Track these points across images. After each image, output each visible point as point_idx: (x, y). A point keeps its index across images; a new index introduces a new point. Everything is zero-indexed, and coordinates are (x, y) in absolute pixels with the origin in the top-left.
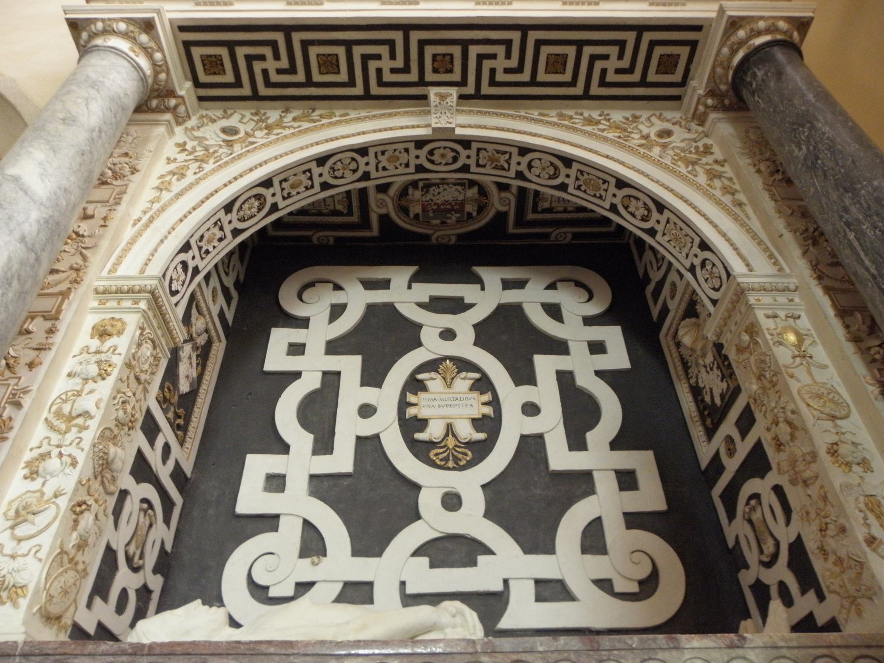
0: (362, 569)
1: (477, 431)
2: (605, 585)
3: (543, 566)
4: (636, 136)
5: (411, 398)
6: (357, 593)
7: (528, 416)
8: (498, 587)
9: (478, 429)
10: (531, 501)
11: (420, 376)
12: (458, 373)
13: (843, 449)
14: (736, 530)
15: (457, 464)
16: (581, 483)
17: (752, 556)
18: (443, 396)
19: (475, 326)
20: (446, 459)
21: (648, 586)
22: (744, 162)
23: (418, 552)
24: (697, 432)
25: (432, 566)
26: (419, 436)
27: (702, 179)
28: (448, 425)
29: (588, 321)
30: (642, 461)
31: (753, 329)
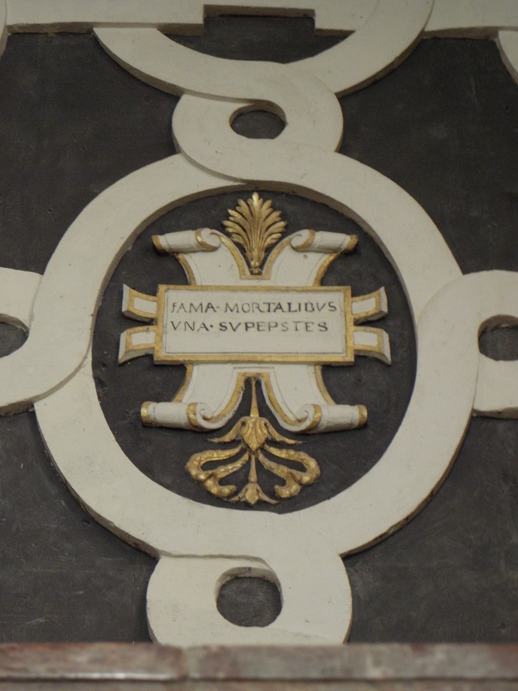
1: (338, 400)
7: (496, 358)
9: (338, 399)
12: (285, 233)
15: (272, 494)
18: (235, 298)
19: (344, 97)
20: (239, 480)
28: (248, 382)
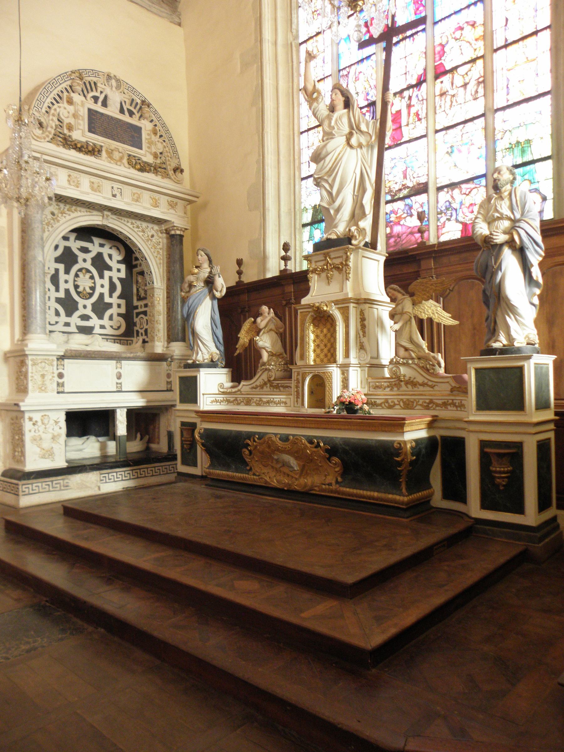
0: (68, 320)
2: (112, 327)
3: (101, 322)
4: (146, 235)
5: (76, 279)
6: (67, 324)
8: (93, 325)
10: (100, 308)
11: (78, 273)
14: (136, 320)
16: (110, 305)
17: (138, 326)
21: (119, 328)
22: (165, 253)
23: (79, 317)
24: (135, 298)
26: (79, 290)
27: (155, 254)
29: (119, 262)
30: (123, 302)
31: (153, 295)
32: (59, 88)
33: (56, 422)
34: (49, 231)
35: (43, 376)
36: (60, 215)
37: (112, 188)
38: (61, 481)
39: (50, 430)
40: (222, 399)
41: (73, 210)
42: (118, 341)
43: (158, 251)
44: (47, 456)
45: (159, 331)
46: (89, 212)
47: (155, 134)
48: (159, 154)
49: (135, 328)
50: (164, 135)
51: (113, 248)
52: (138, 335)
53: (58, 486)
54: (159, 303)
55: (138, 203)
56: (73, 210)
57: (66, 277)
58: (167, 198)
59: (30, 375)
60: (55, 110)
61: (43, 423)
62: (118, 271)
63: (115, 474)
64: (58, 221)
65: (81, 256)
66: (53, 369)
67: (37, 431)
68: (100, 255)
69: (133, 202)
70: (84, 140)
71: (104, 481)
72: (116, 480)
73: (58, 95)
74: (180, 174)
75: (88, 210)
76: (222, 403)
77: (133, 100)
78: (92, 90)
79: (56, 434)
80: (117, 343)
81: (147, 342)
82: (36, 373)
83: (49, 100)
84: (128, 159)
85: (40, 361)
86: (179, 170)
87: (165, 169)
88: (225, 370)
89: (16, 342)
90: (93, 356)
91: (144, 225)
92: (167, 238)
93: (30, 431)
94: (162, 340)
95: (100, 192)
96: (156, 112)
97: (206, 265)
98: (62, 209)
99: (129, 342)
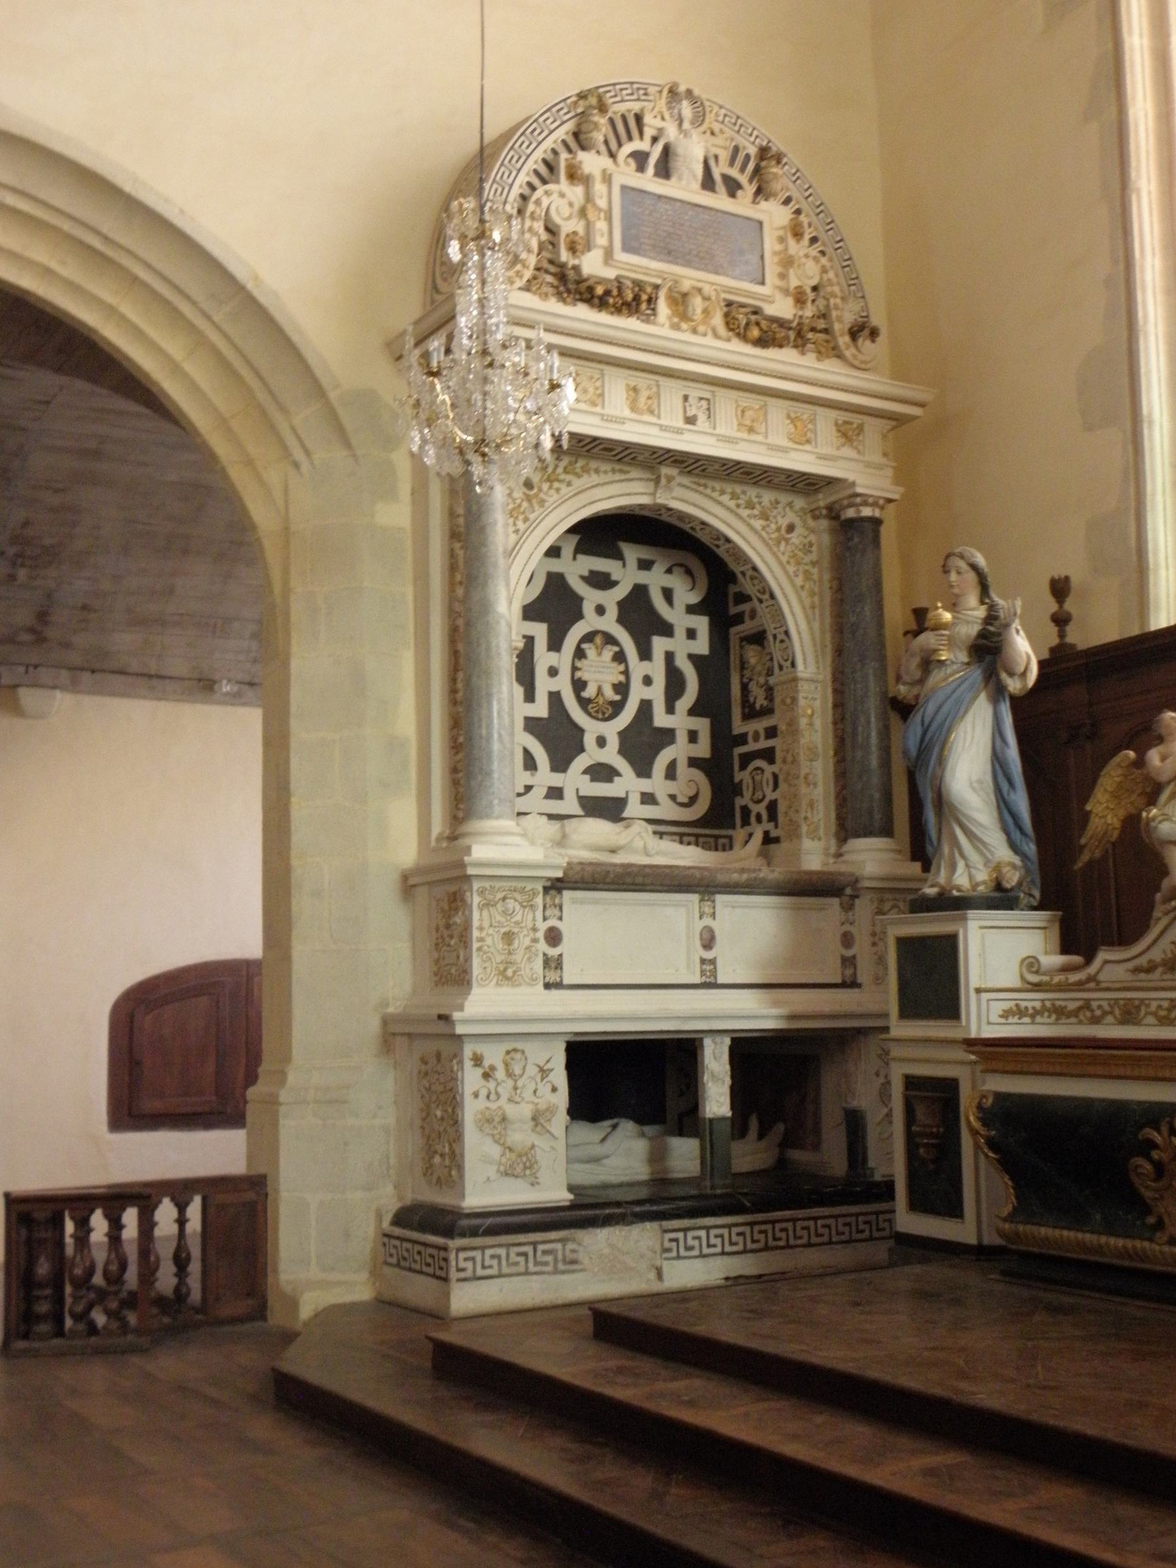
0: (556, 780)
2: (673, 797)
3: (645, 785)
4: (773, 526)
6: (555, 793)
8: (623, 795)
11: (584, 646)
13: (811, 777)
14: (742, 776)
16: (668, 736)
17: (747, 794)
21: (693, 800)
22: (827, 577)
23: (585, 772)
24: (737, 712)
25: (592, 780)
26: (585, 694)
27: (799, 581)
29: (691, 609)
30: (702, 725)
31: (794, 700)
32: (548, 144)
33: (544, 1072)
34: (516, 531)
35: (508, 937)
36: (545, 486)
37: (686, 398)
38: (559, 1246)
39: (528, 1094)
40: (1038, 1005)
41: (578, 470)
42: (692, 839)
43: (806, 572)
44: (519, 1169)
45: (811, 805)
46: (621, 471)
47: (797, 234)
48: (808, 290)
49: (739, 802)
50: (823, 236)
51: (675, 569)
52: (746, 822)
53: (550, 1258)
54: (811, 724)
55: (754, 437)
56: (578, 470)
57: (552, 658)
58: (833, 414)
59: (476, 934)
60: (538, 202)
61: (510, 1074)
62: (688, 637)
63: (703, 1233)
64: (542, 502)
65: (591, 597)
66: (534, 920)
67: (493, 1097)
68: (640, 592)
69: (739, 435)
70: (610, 274)
71: (674, 1254)
72: (706, 1251)
73: (545, 161)
74: (868, 342)
75: (617, 467)
76: (1038, 1019)
77: (736, 150)
78: (630, 138)
79: (542, 1106)
80: (689, 844)
81: (777, 840)
82: (491, 931)
83: (523, 178)
84: (726, 315)
85: (500, 895)
86: (866, 332)
87: (826, 331)
88: (1040, 917)
89: (433, 844)
90: (639, 880)
91: (768, 497)
92: (832, 531)
93: (476, 1095)
94: (821, 832)
95: (651, 412)
96: (797, 176)
97: (972, 599)
98: (550, 470)
99: (721, 841)
